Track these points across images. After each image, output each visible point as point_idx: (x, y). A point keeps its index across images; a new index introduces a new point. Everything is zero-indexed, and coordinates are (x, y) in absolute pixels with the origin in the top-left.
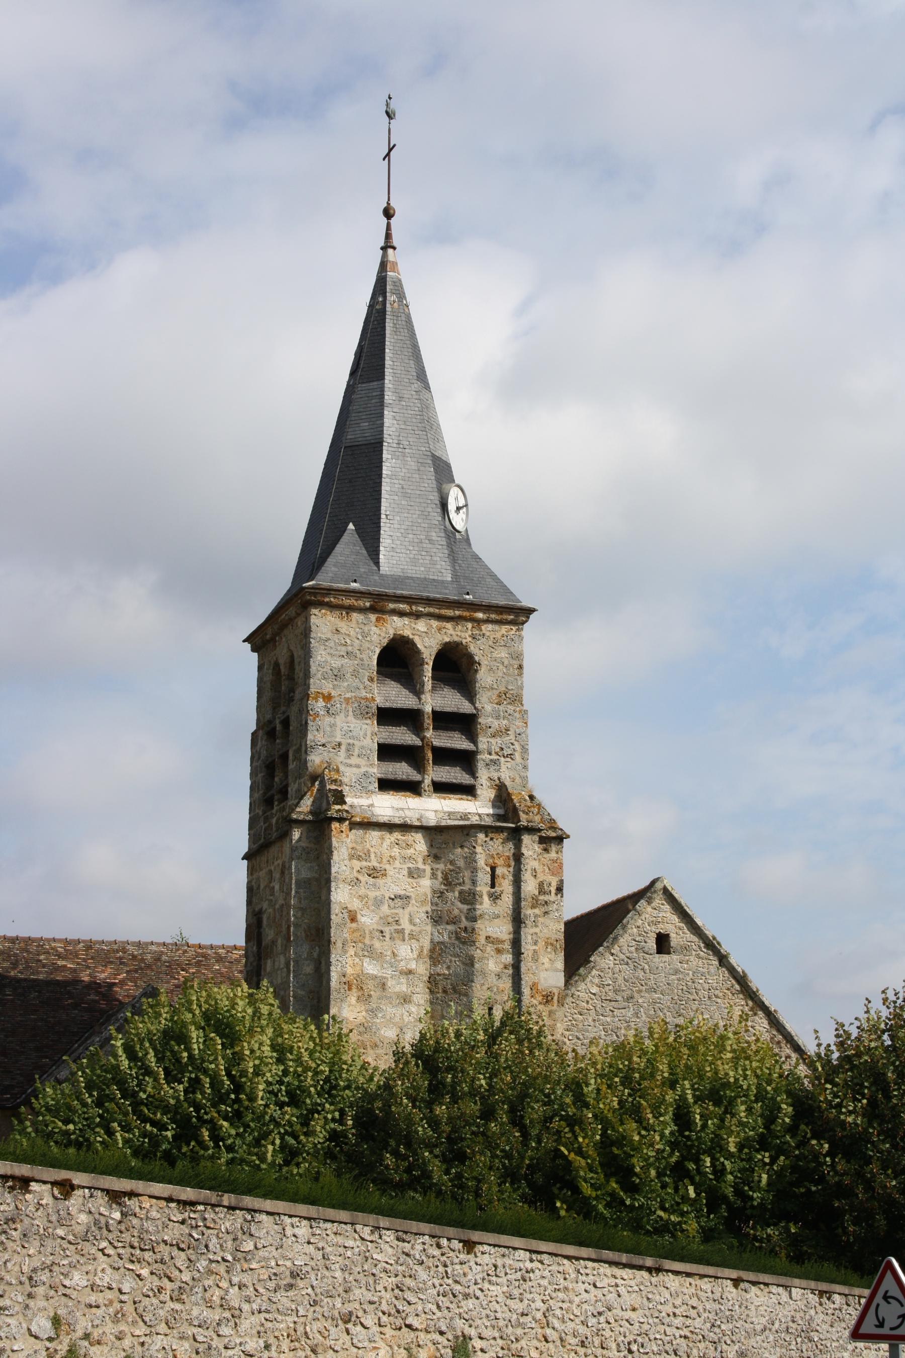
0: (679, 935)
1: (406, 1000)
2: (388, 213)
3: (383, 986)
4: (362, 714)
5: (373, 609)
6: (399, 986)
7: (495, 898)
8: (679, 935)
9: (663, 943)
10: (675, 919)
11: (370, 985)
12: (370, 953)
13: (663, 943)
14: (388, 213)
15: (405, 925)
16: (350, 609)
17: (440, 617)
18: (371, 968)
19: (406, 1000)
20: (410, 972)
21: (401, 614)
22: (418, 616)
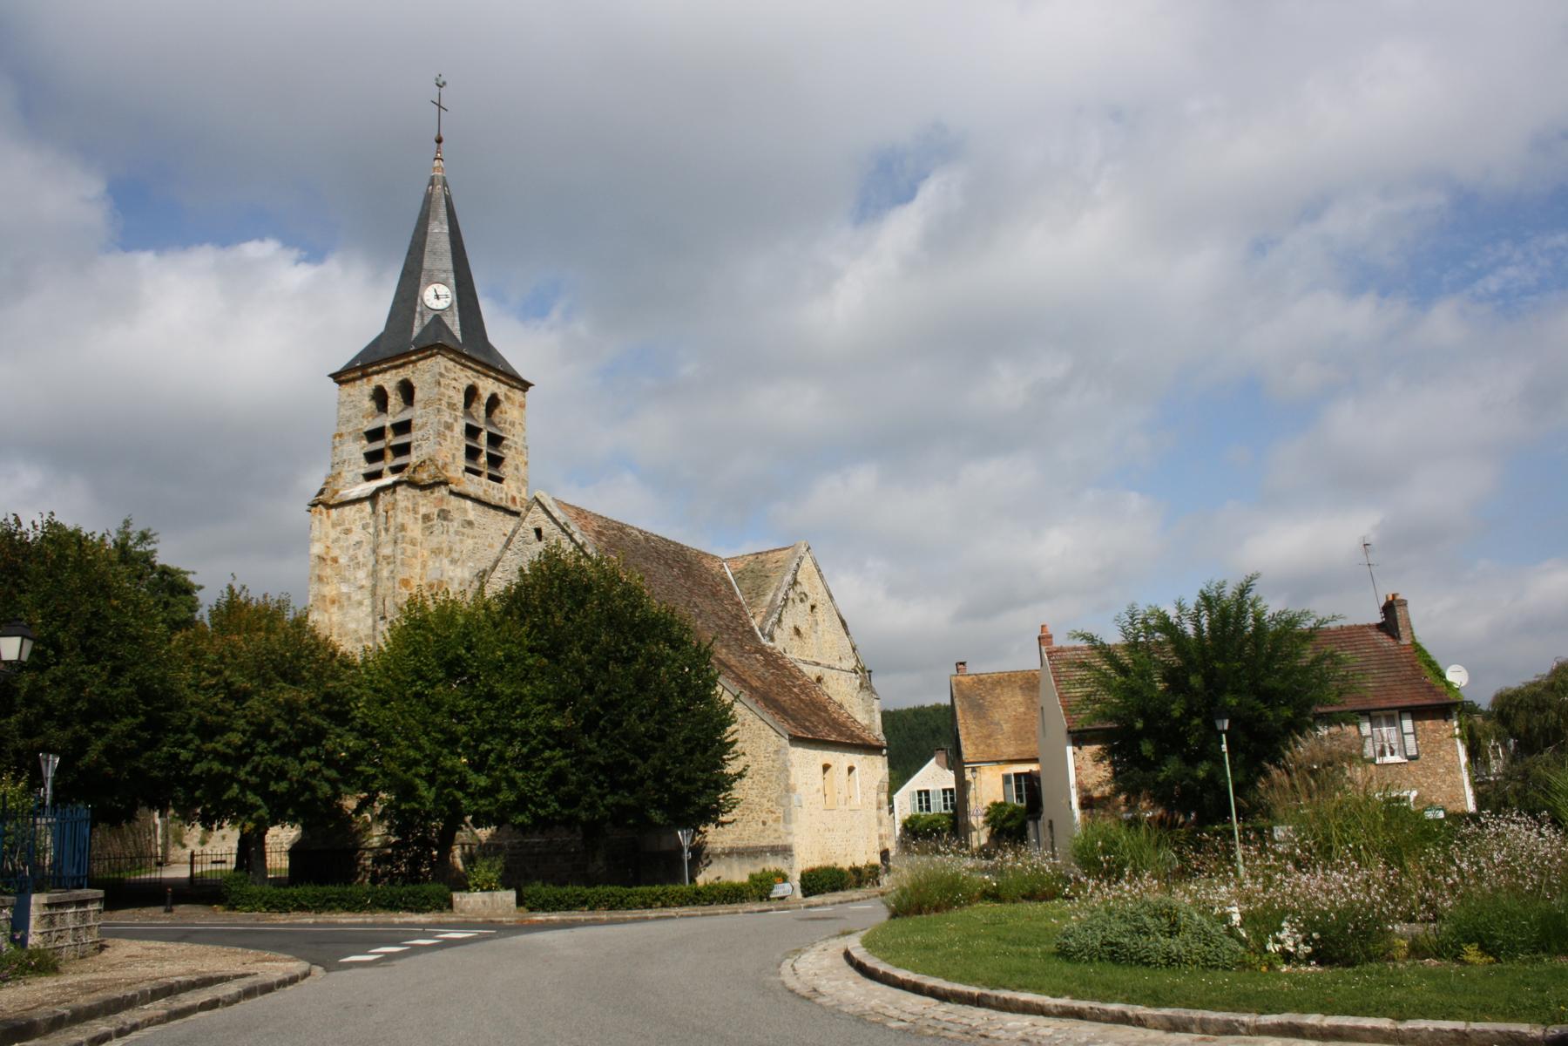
0: (548, 528)
1: (360, 603)
2: (439, 141)
3: (349, 598)
4: (357, 439)
5: (365, 375)
6: (357, 596)
7: (387, 530)
8: (548, 528)
9: (538, 532)
10: (545, 516)
11: (344, 598)
12: (344, 580)
13: (538, 532)
14: (439, 141)
15: (361, 559)
16: (354, 380)
17: (396, 367)
18: (344, 589)
19: (360, 603)
20: (362, 587)
21: (377, 373)
22: (385, 371)
